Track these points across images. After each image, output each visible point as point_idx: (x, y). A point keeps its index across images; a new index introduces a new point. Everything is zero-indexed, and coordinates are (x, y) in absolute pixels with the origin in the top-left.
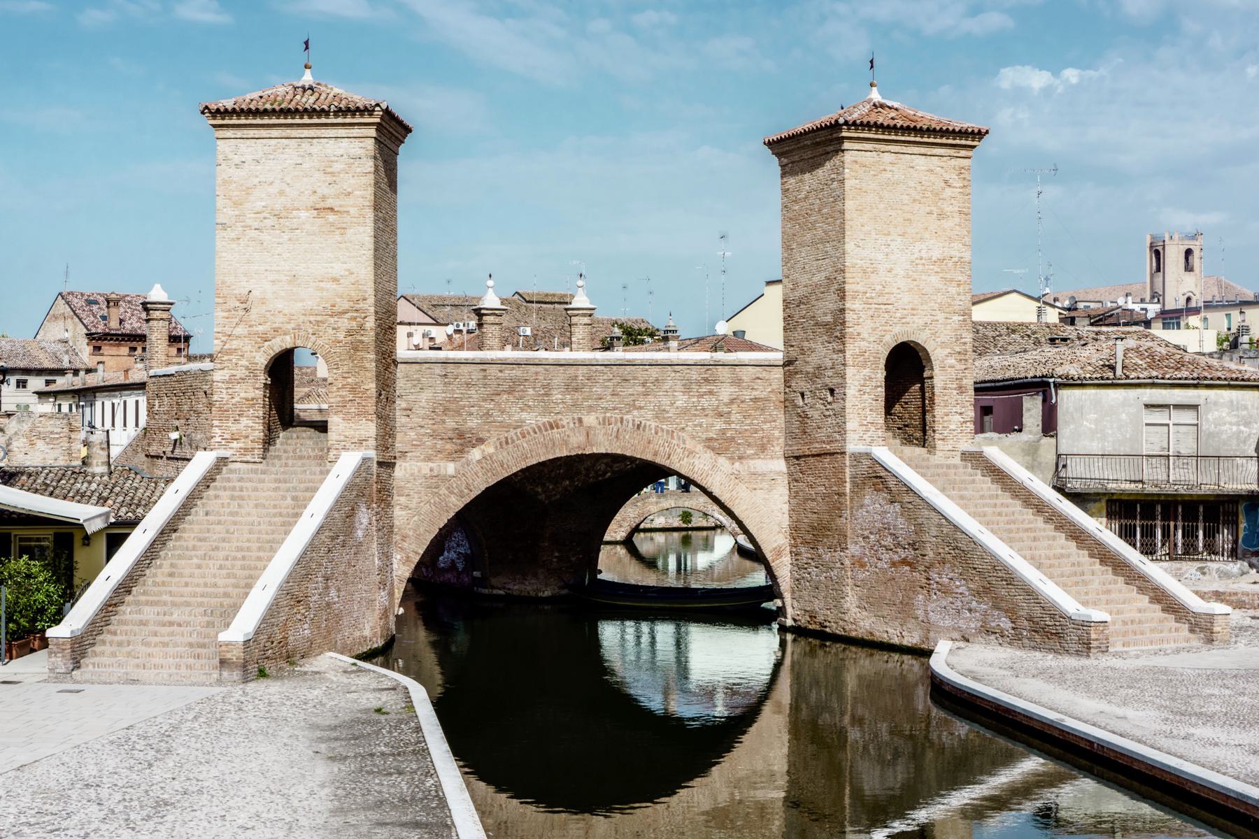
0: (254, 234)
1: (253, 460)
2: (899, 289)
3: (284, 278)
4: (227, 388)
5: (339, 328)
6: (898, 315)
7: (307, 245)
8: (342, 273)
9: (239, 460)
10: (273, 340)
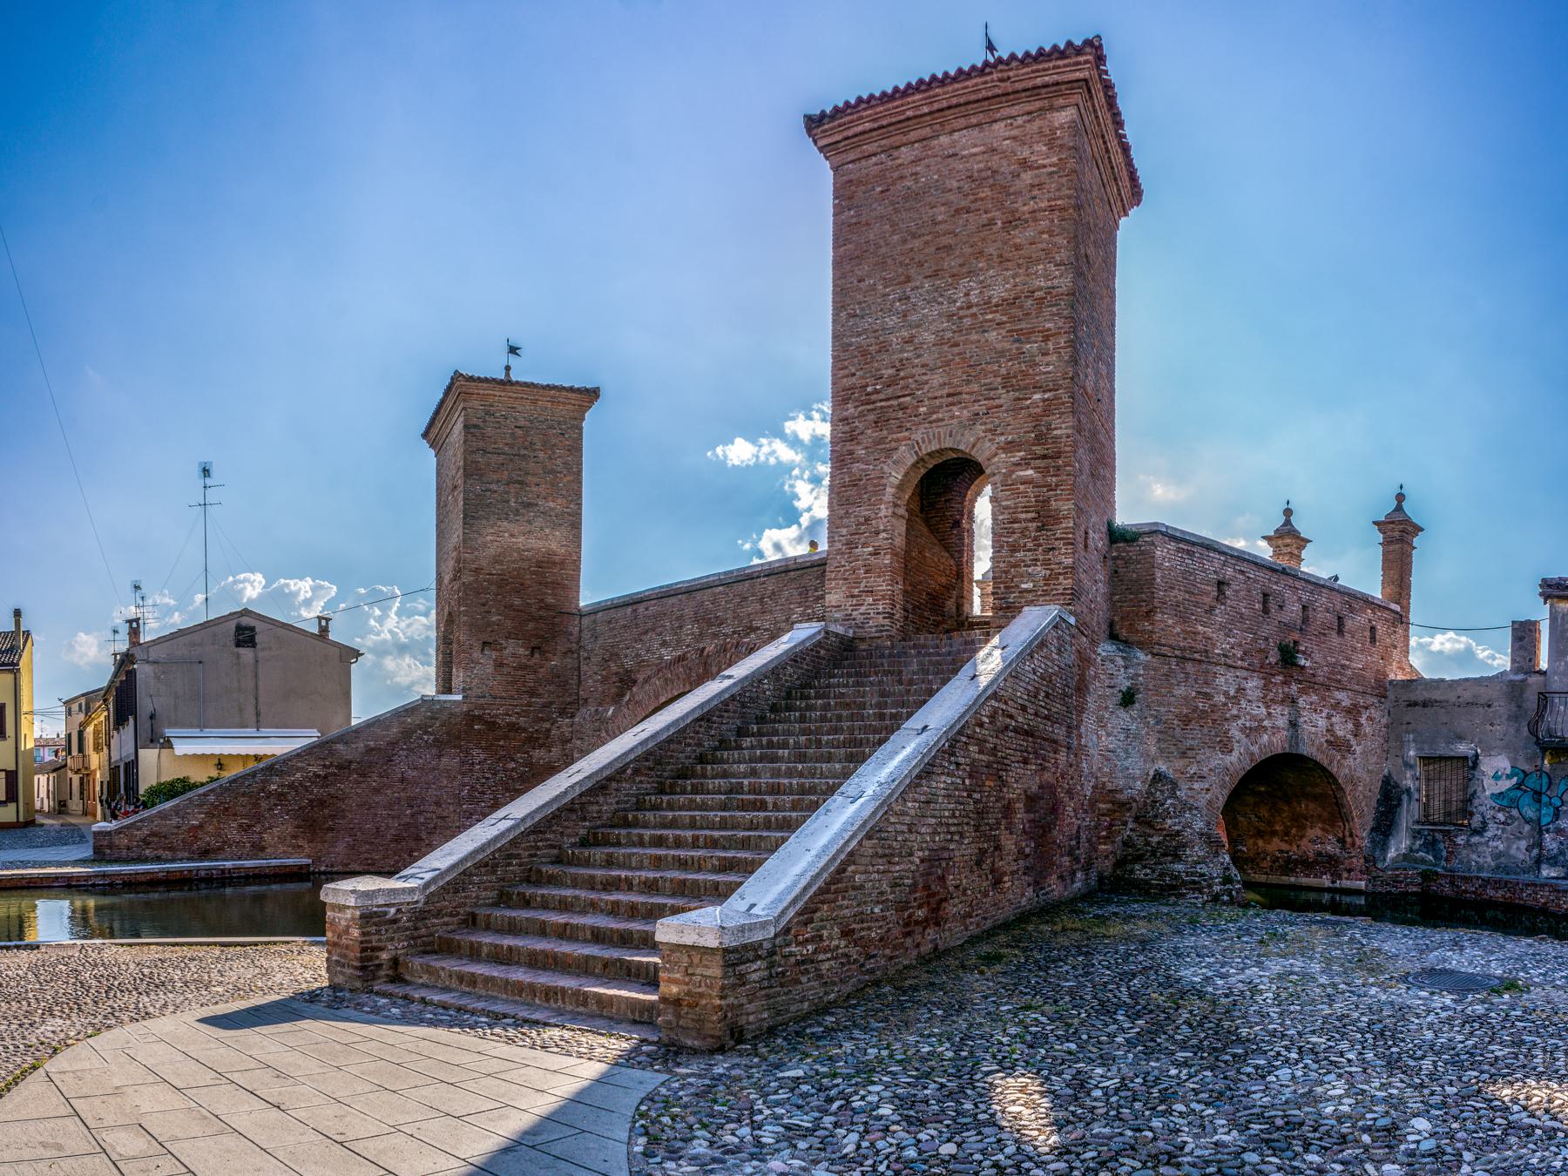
2: (923, 366)
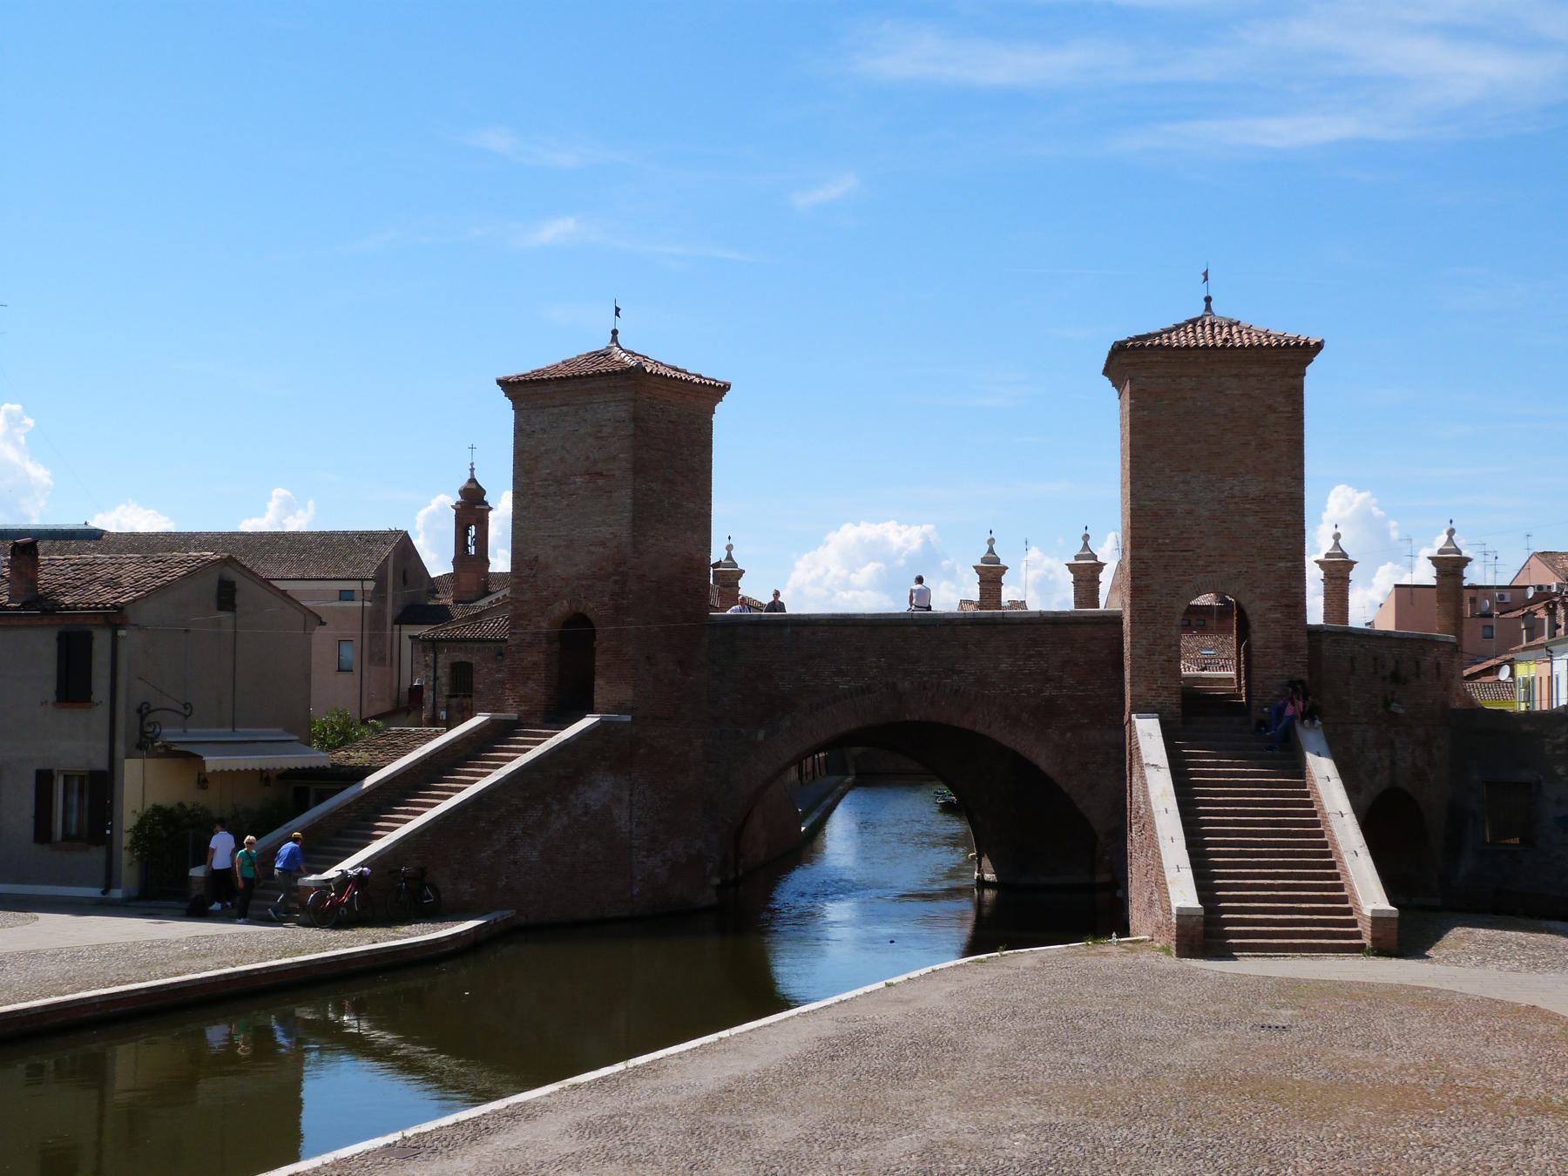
6: (1201, 563)
8: (607, 537)
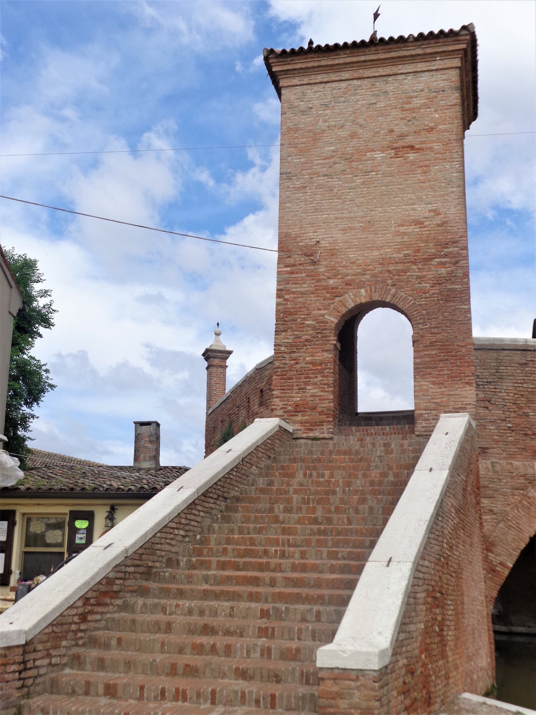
0: (322, 180)
1: (321, 436)
3: (358, 225)
4: (290, 353)
5: (424, 276)
7: (384, 188)
8: (426, 214)
9: (305, 435)
10: (346, 296)
